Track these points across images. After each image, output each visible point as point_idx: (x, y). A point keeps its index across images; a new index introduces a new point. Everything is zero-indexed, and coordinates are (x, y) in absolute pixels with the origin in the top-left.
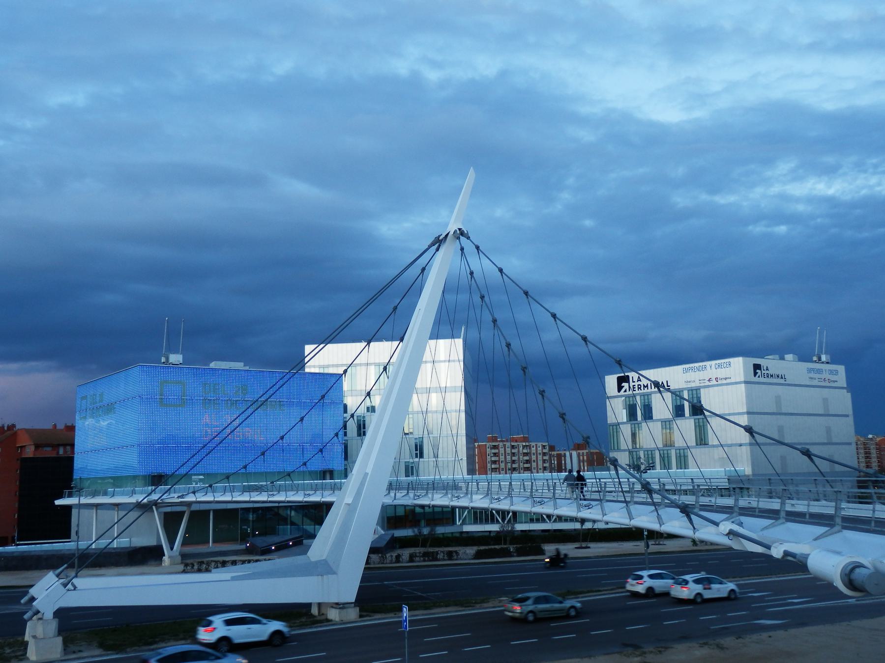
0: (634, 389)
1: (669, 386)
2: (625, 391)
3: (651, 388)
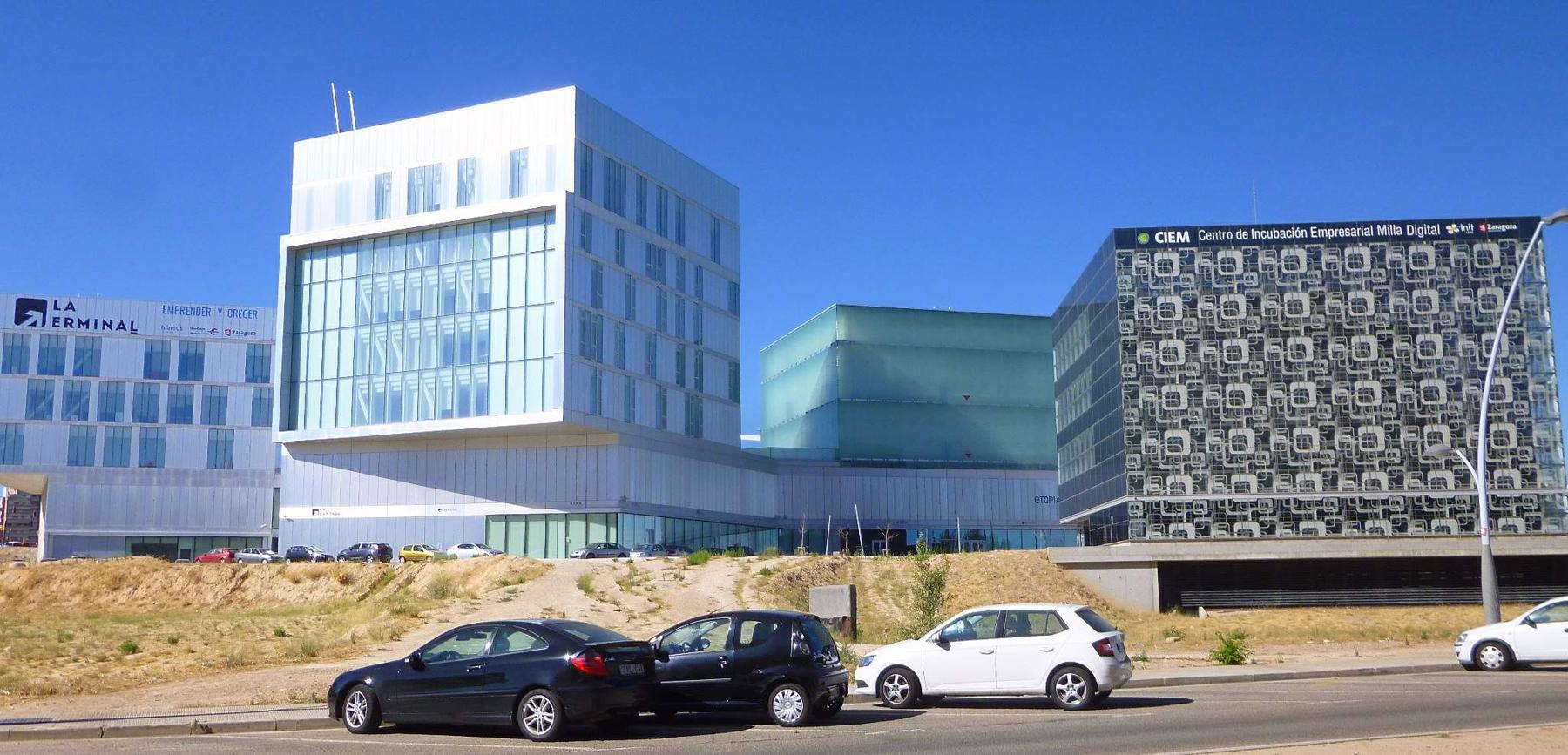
2: (34, 324)
3: (96, 328)
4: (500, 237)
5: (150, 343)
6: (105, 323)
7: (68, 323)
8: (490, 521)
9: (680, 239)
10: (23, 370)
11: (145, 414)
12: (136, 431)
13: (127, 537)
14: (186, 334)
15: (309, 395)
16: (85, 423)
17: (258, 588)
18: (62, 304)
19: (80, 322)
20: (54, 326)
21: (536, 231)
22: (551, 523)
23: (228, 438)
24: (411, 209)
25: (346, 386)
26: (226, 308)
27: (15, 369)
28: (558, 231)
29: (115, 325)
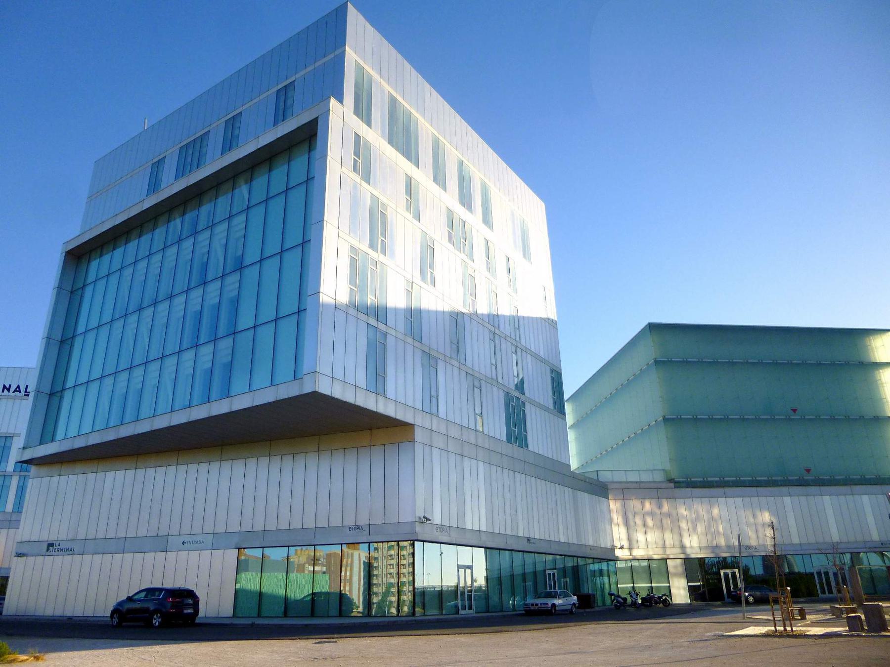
1: (29, 392)
9: (487, 220)
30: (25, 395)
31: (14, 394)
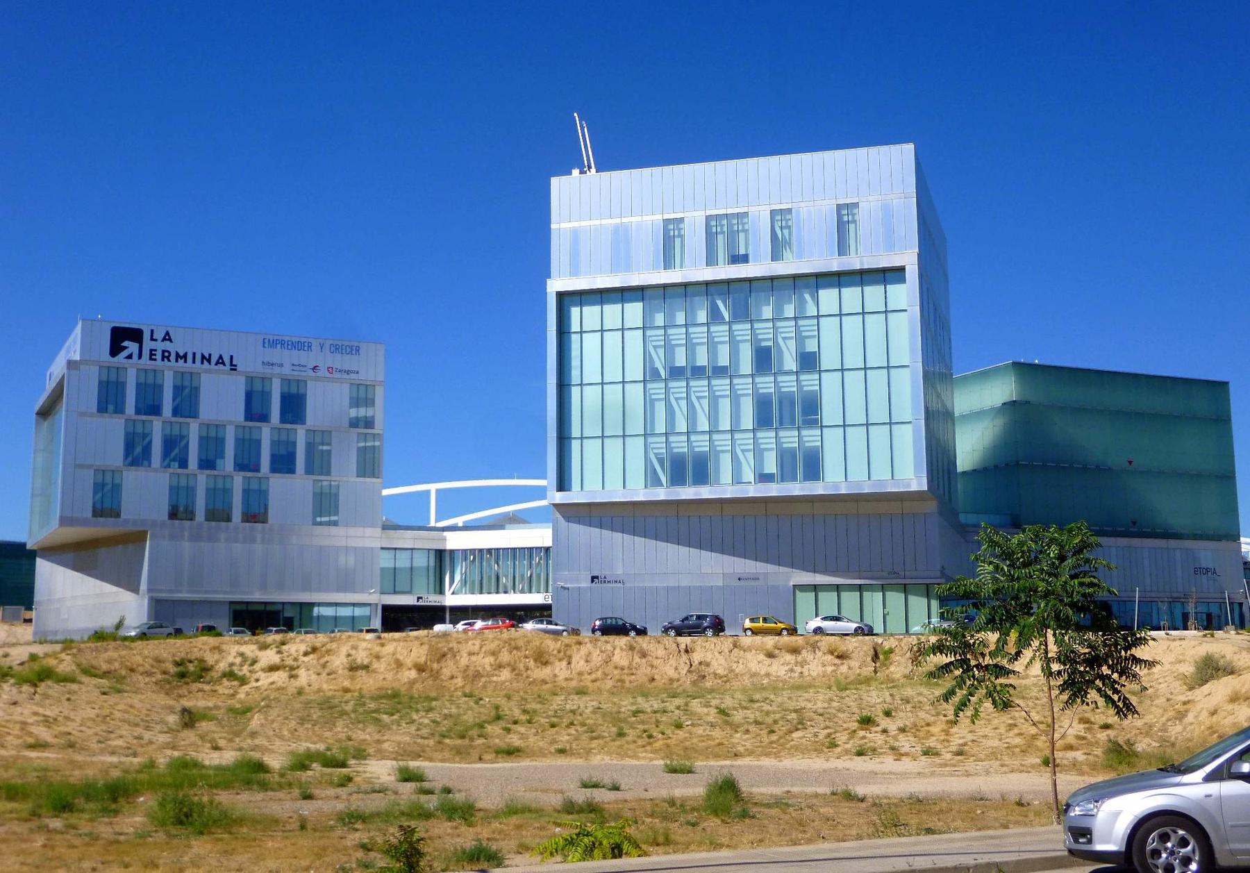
0: (153, 357)
1: (236, 366)
2: (130, 357)
3: (194, 362)
4: (828, 296)
5: (250, 379)
6: (203, 357)
7: (166, 356)
8: (797, 592)
10: (119, 410)
11: (247, 464)
12: (238, 481)
13: (231, 603)
14: (286, 370)
15: (586, 456)
16: (185, 471)
17: (723, 662)
18: (159, 335)
19: (178, 356)
20: (151, 359)
21: (874, 293)
22: (865, 594)
23: (190, 485)
24: (711, 260)
25: (636, 446)
26: (328, 343)
27: (111, 408)
28: (905, 295)
29: (214, 360)
30: (232, 369)
31: (216, 367)
